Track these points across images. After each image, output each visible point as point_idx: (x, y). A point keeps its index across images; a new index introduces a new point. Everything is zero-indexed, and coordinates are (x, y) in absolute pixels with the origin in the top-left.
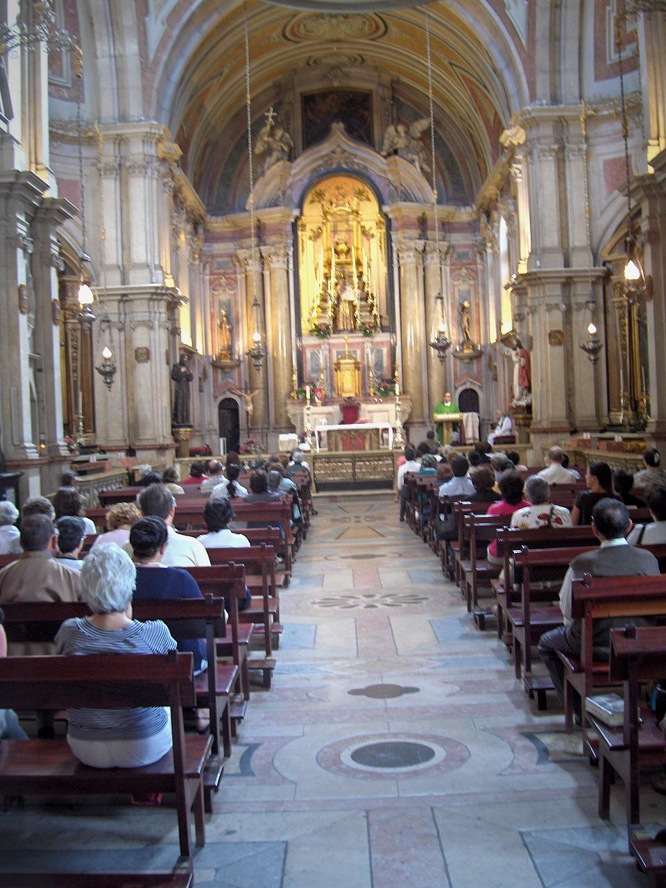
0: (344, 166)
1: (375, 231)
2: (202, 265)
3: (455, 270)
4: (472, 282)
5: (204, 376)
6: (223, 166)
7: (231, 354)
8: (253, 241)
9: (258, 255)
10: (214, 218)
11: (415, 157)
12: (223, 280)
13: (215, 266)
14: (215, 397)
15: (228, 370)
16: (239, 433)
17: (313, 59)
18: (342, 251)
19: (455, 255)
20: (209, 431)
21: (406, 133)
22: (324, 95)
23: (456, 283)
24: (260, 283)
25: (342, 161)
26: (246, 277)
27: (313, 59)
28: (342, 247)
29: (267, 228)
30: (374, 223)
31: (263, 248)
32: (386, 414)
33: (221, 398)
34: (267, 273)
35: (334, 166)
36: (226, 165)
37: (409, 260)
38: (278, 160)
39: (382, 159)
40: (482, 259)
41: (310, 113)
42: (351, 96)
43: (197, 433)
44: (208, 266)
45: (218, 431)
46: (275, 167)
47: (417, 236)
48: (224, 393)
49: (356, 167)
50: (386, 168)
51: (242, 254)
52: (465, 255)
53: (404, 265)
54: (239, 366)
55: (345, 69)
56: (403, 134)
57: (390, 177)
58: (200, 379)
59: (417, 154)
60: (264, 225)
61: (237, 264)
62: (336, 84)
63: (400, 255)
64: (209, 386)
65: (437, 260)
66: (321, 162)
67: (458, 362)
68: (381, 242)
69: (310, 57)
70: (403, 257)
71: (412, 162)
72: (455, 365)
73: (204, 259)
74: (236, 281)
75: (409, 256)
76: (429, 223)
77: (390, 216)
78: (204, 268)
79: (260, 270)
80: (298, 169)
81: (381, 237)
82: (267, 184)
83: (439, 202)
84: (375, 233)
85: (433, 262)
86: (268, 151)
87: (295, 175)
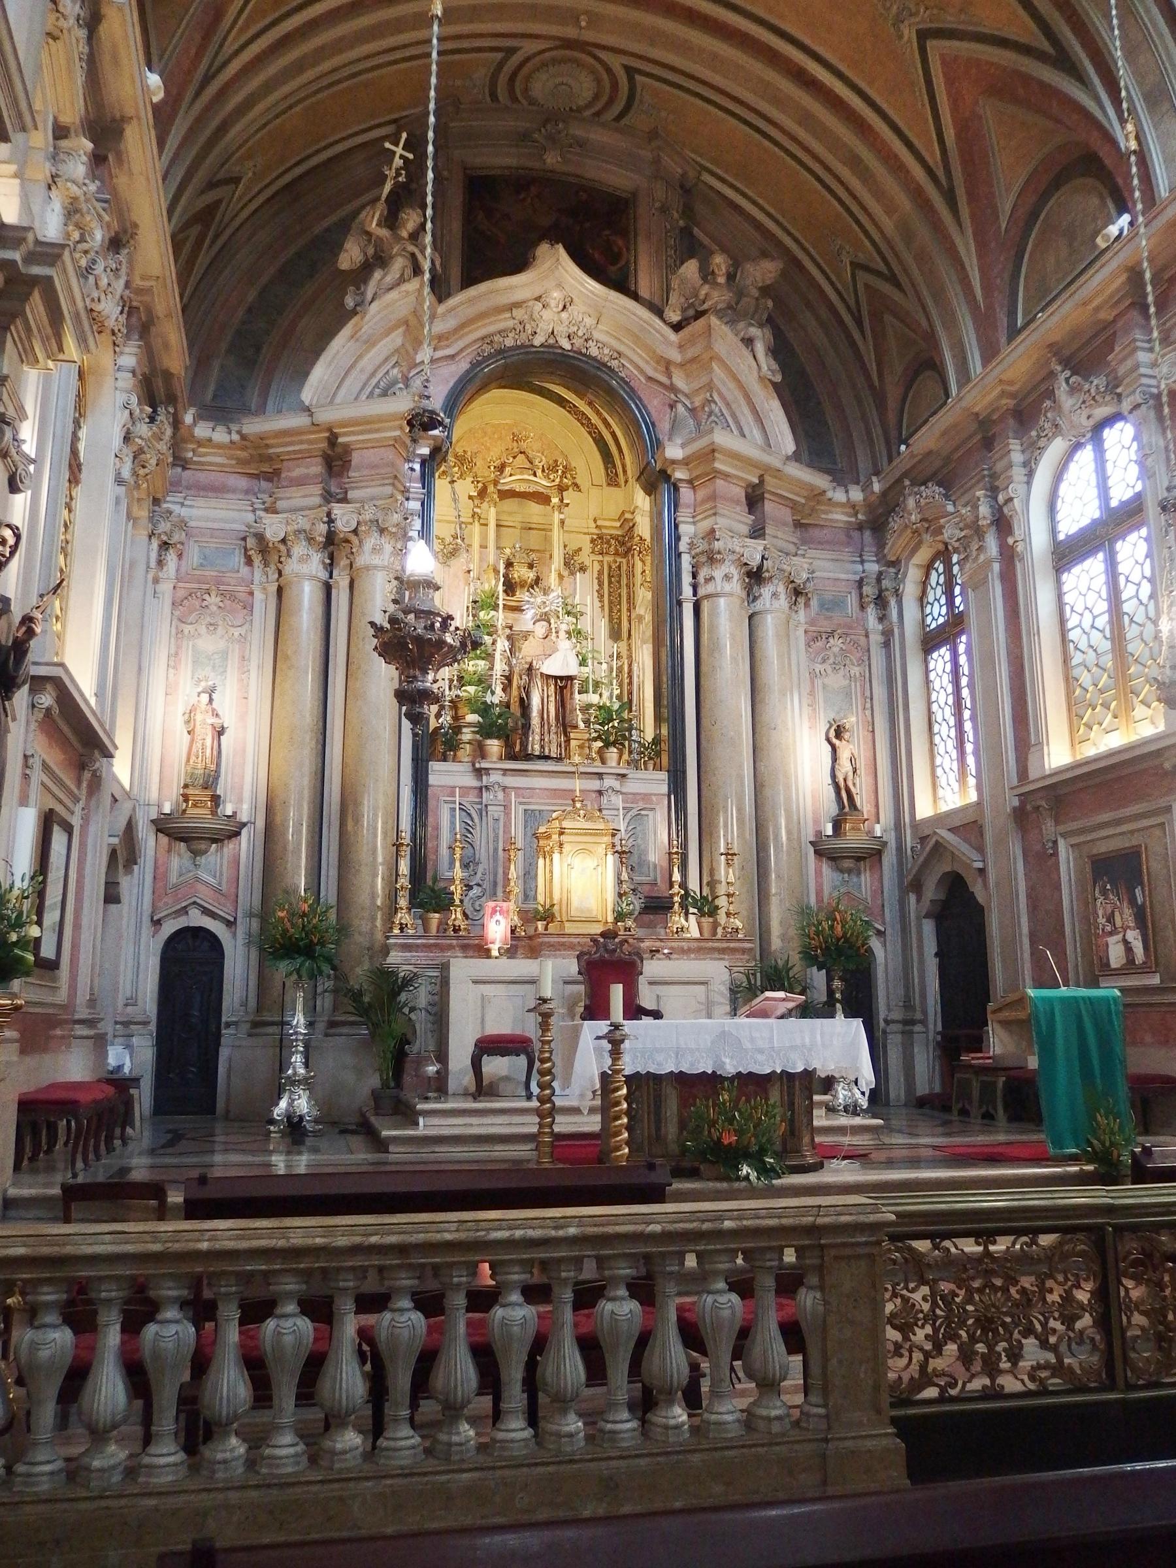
0: (567, 346)
1: (586, 557)
2: (155, 544)
3: (815, 639)
4: (856, 670)
5: (124, 855)
6: (240, 313)
7: (216, 800)
8: (311, 496)
9: (323, 528)
10: (202, 430)
11: (754, 331)
12: (213, 600)
13: (193, 554)
14: (157, 923)
15: (203, 846)
16: (218, 1036)
17: (516, 59)
18: (523, 584)
19: (814, 603)
20: (126, 1024)
21: (731, 277)
22: (522, 183)
23: (819, 667)
24: (319, 610)
25: (562, 330)
26: (280, 590)
27: (516, 59)
28: (521, 572)
29: (356, 457)
30: (588, 538)
31: (338, 510)
32: (703, 987)
33: (170, 927)
34: (341, 581)
35: (537, 342)
36: (249, 310)
37: (727, 588)
38: (402, 280)
39: (668, 331)
40: (881, 619)
41: (481, 215)
42: (583, 196)
43: (81, 1031)
44: (171, 557)
45: (153, 1027)
46: (393, 295)
47: (745, 530)
48: (184, 911)
49: (594, 351)
50: (675, 356)
51: (274, 528)
52: (835, 604)
53: (708, 596)
54: (238, 834)
55: (578, 131)
56: (721, 280)
57: (679, 381)
58: (113, 854)
59: (761, 326)
60: (347, 450)
61: (257, 560)
62: (552, 159)
63: (703, 573)
64: (137, 887)
65: (783, 602)
66: (510, 324)
67: (826, 868)
68: (601, 584)
69: (511, 51)
70: (711, 578)
71: (749, 342)
72: (819, 873)
73: (164, 526)
74: (249, 607)
75: (727, 577)
76: (769, 506)
77: (679, 474)
78: (160, 563)
79: (323, 575)
80: (451, 323)
81: (600, 573)
82: (371, 343)
83: (796, 457)
84: (587, 563)
85: (776, 604)
86: (379, 260)
87: (440, 338)
